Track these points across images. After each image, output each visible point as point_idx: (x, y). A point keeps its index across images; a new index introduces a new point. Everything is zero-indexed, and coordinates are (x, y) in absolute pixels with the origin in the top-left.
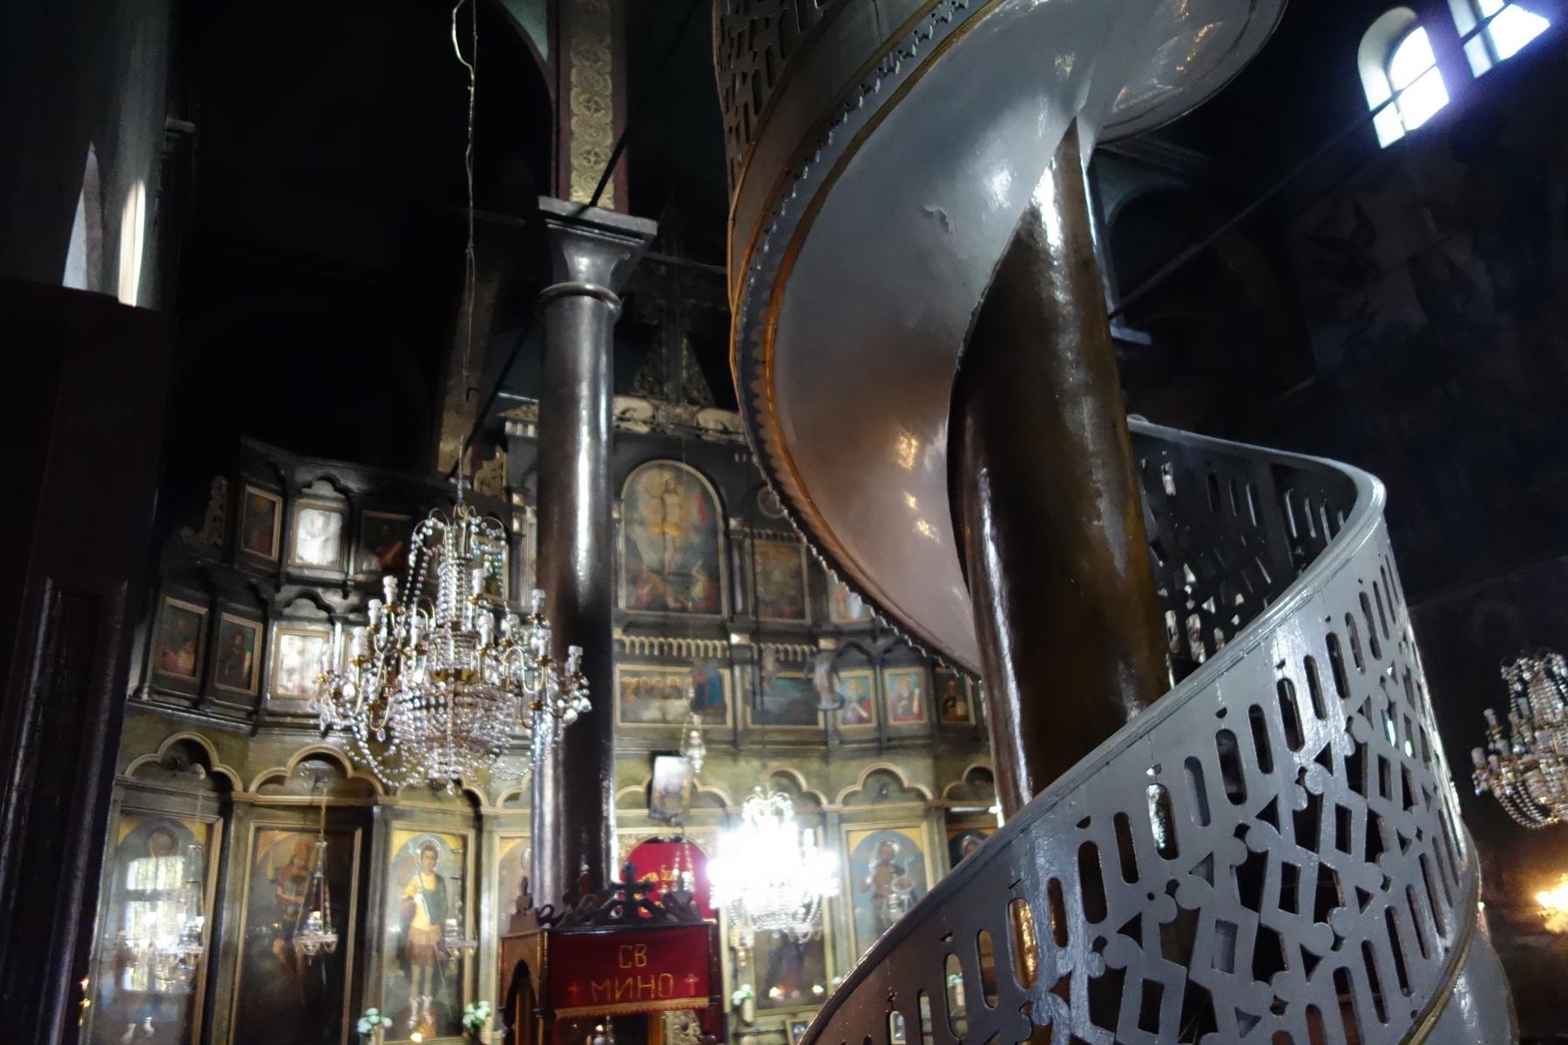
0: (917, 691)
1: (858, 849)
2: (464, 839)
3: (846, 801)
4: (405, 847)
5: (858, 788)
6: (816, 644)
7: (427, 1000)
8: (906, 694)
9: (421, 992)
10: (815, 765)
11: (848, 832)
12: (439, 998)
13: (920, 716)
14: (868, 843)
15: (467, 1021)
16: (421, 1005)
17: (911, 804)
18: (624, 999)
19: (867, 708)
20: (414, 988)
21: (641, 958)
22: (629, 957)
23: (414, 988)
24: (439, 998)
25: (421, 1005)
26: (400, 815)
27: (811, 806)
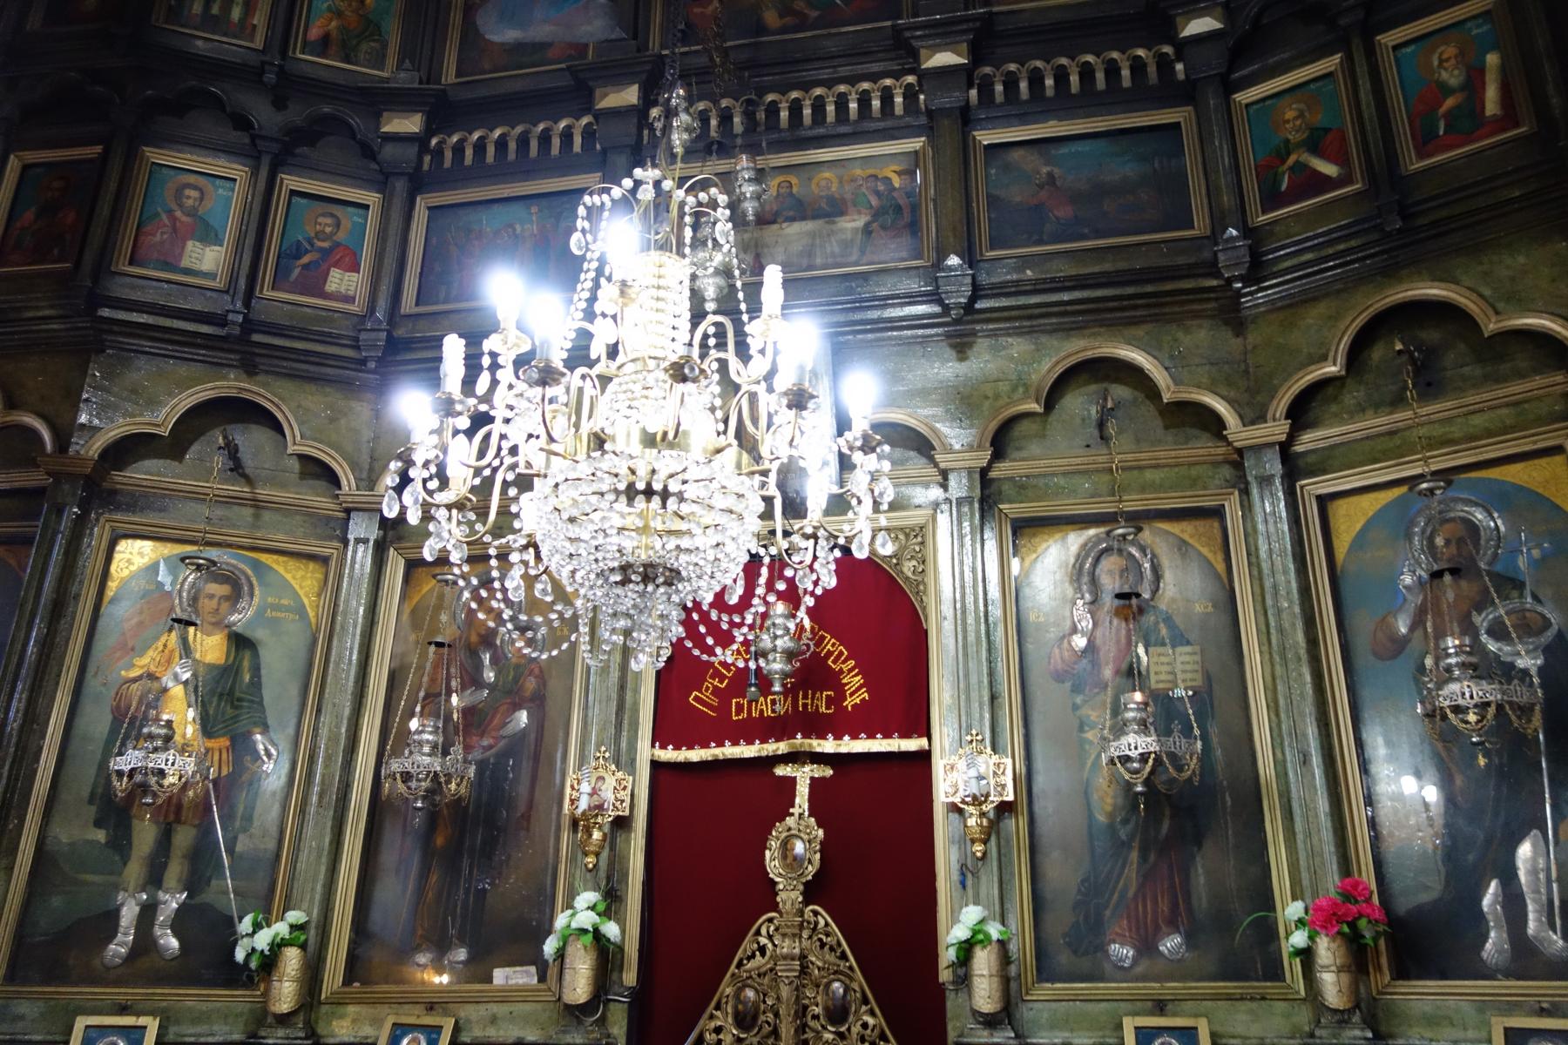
0: (1492, 59)
1: (1360, 541)
2: (324, 560)
3: (1301, 413)
4: (153, 568)
5: (1331, 369)
6: (1170, 35)
7: (172, 902)
8: (1452, 77)
9: (154, 880)
10: (1201, 337)
11: (1323, 501)
12: (208, 896)
13: (1509, 117)
14: (1396, 523)
16: (148, 913)
17: (1517, 388)
19: (1340, 158)
20: (135, 870)
23: (135, 870)
24: (208, 896)
25: (148, 913)
26: (136, 501)
27: (1203, 448)
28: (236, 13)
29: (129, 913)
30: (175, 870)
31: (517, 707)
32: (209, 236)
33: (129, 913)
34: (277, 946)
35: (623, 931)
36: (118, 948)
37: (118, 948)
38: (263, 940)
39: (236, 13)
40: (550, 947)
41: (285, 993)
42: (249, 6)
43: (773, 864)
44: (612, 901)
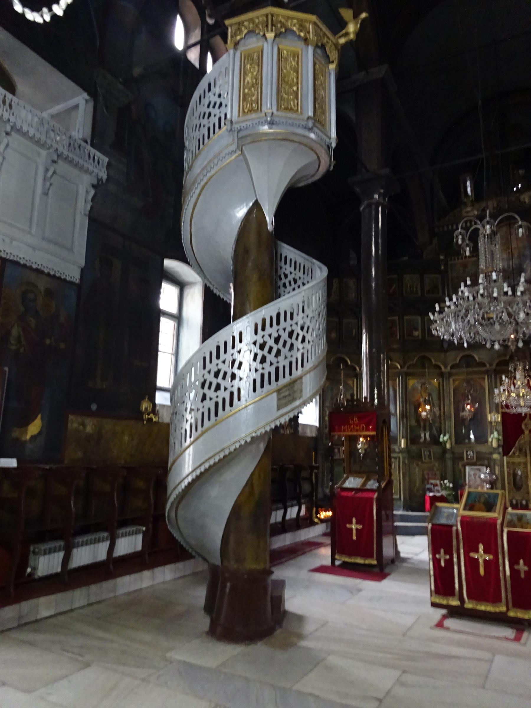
9: (425, 430)
15: (441, 440)
18: (351, 431)
20: (422, 429)
21: (356, 420)
22: (353, 420)
23: (422, 429)
28: (415, 289)
29: (422, 435)
30: (427, 429)
31: (476, 403)
32: (417, 329)
33: (422, 435)
34: (447, 439)
35: (501, 438)
36: (422, 440)
37: (422, 440)
38: (446, 438)
39: (415, 289)
40: (490, 440)
41: (448, 446)
42: (417, 288)
43: (523, 427)
44: (499, 434)
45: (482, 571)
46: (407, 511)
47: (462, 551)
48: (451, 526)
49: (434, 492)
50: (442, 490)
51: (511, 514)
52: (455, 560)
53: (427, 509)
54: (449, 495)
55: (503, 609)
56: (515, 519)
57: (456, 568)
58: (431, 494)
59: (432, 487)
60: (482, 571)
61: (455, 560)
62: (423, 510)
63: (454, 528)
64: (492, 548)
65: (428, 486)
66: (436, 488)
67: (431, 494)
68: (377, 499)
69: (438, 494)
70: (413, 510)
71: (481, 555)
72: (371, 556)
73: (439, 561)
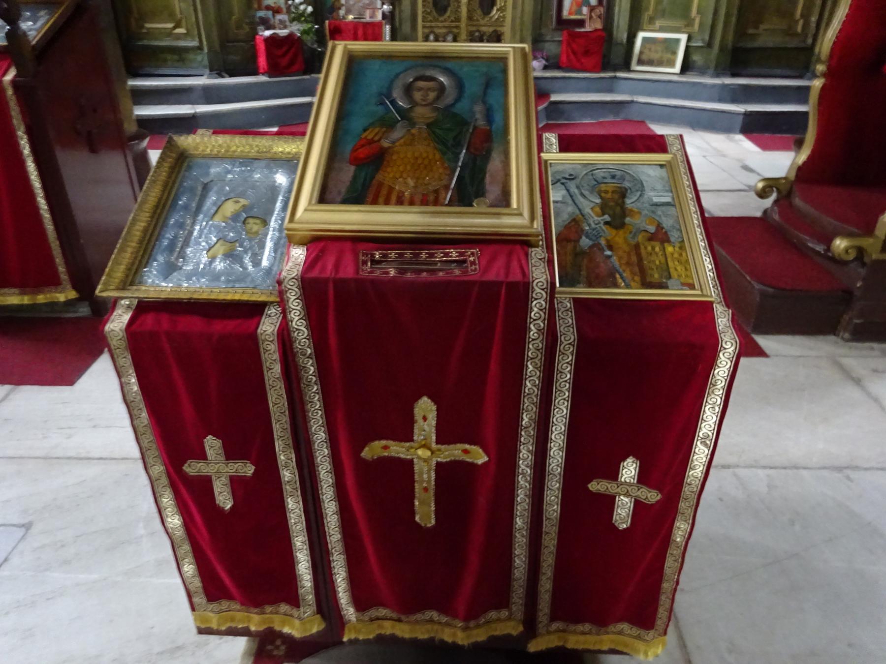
45: (425, 513)
46: (221, 76)
47: (319, 436)
48: (256, 309)
49: (274, 28)
50: (292, 20)
51: (566, 179)
52: (288, 475)
53: (262, 71)
54: (305, 32)
55: (514, 629)
56: (589, 204)
57: (294, 506)
58: (267, 33)
59: (270, 13)
60: (425, 513)
61: (288, 475)
62: (255, 73)
63: (268, 327)
64: (482, 409)
65: (261, 14)
66: (279, 17)
67: (267, 33)
68: (13, 82)
69: (283, 32)
70: (232, 75)
71: (424, 448)
72: (53, 282)
73: (204, 485)
